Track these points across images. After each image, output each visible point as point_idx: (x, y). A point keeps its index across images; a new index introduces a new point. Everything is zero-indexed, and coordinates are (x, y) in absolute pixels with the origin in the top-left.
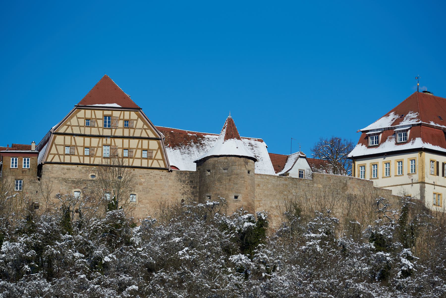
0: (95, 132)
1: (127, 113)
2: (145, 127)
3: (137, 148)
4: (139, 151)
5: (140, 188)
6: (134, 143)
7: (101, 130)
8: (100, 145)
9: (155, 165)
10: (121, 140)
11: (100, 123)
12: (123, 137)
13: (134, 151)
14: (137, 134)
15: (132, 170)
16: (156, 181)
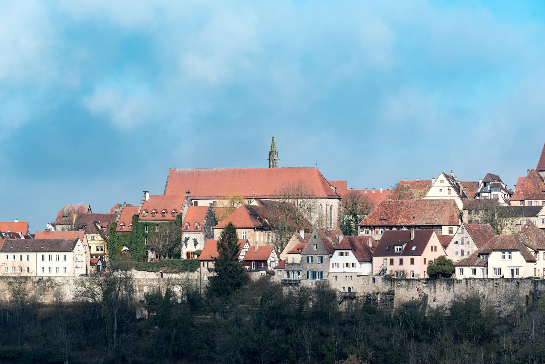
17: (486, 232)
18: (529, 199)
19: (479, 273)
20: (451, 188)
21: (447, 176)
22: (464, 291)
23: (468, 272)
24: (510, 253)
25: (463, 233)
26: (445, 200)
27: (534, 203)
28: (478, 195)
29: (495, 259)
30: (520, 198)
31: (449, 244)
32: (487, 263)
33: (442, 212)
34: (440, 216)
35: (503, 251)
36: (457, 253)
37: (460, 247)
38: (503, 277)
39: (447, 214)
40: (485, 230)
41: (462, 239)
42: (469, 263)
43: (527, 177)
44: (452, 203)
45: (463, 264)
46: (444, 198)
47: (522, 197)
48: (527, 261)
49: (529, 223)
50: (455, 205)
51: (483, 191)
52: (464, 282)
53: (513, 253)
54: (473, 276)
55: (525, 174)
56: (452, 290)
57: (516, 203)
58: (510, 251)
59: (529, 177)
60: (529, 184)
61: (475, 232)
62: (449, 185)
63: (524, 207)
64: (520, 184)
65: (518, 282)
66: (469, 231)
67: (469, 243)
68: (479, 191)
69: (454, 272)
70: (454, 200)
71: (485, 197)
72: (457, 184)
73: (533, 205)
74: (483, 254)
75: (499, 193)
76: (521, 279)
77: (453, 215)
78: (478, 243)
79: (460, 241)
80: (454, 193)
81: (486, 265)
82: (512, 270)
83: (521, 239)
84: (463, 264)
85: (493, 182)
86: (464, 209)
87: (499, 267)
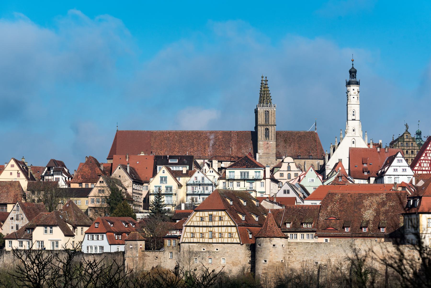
0: (204, 224)
1: (220, 212)
2: (229, 220)
3: (225, 232)
4: (226, 234)
5: (227, 255)
6: (224, 229)
7: (207, 222)
8: (207, 231)
9: (235, 241)
10: (217, 228)
11: (207, 219)
12: (218, 226)
13: (224, 234)
14: (225, 224)
15: (223, 245)
16: (235, 251)
17: (39, 210)
18: (87, 182)
19: (26, 245)
20: (20, 172)
21: (17, 162)
22: (11, 261)
23: (16, 244)
24: (51, 228)
25: (18, 210)
26: (12, 182)
27: (90, 185)
28: (43, 177)
29: (39, 233)
30: (79, 181)
31: (6, 219)
32: (32, 237)
33: (7, 192)
34: (6, 196)
35: (45, 226)
36: (12, 228)
37: (15, 222)
38: (45, 249)
39: (12, 194)
40: (38, 208)
41: (17, 216)
42: (16, 237)
43: (86, 163)
44: (17, 184)
45: (11, 237)
46: (13, 180)
47: (81, 180)
48: (66, 235)
49: (71, 202)
50: (19, 186)
51: (46, 174)
52: (12, 254)
53: (54, 228)
54: (20, 248)
55: (84, 161)
56: (2, 260)
57: (76, 186)
58: (51, 226)
59: (87, 163)
60: (87, 169)
61: (29, 210)
62: (18, 169)
63: (82, 188)
64: (80, 170)
65: (55, 254)
66: (23, 208)
67: (22, 219)
68: (43, 174)
69: (4, 245)
70: (19, 182)
71: (48, 179)
72: (27, 168)
73: (90, 187)
74: (29, 229)
75: (60, 177)
76: (60, 251)
77: (17, 195)
78: (29, 218)
79: (15, 217)
80: (22, 175)
81: (30, 238)
82: (53, 243)
83: (62, 216)
84: (11, 237)
85: (57, 166)
86: (28, 190)
87: (42, 240)
